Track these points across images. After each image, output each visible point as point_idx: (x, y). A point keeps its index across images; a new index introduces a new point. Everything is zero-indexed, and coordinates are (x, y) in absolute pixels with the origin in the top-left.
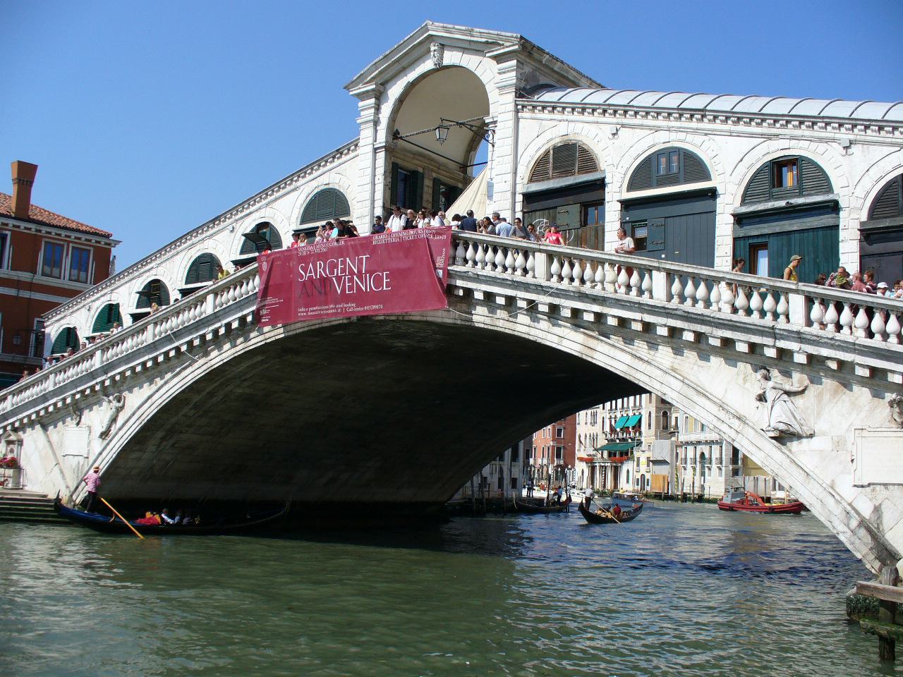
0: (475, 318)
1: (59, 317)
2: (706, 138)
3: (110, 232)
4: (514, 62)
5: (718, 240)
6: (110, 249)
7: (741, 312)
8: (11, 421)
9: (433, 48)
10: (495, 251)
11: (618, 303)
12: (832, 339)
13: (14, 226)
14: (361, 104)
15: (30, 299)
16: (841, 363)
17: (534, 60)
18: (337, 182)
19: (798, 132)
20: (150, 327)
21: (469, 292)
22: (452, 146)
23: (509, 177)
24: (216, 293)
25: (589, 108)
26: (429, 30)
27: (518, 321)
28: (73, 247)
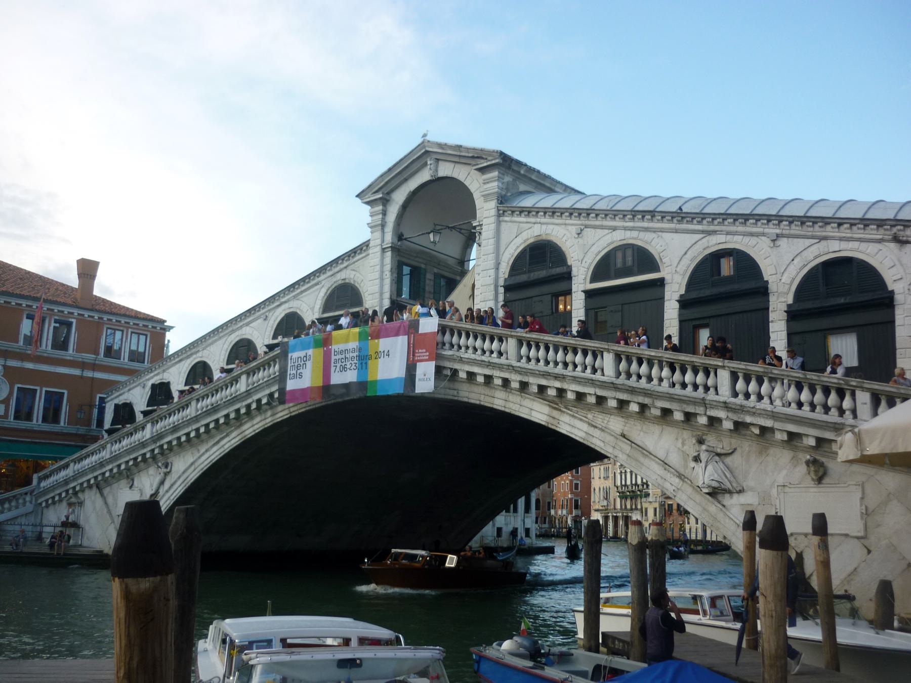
0: (462, 394)
1: (118, 394)
2: (652, 235)
3: (164, 318)
5: (666, 323)
6: (164, 336)
7: (677, 386)
8: (72, 485)
9: (429, 163)
10: (476, 338)
11: (575, 380)
12: (753, 408)
13: (79, 314)
15: (93, 379)
16: (764, 430)
17: (514, 171)
19: (733, 229)
20: (194, 403)
21: (455, 372)
22: (448, 246)
23: (492, 272)
24: (248, 373)
26: (424, 147)
27: (496, 395)
28: (132, 333)
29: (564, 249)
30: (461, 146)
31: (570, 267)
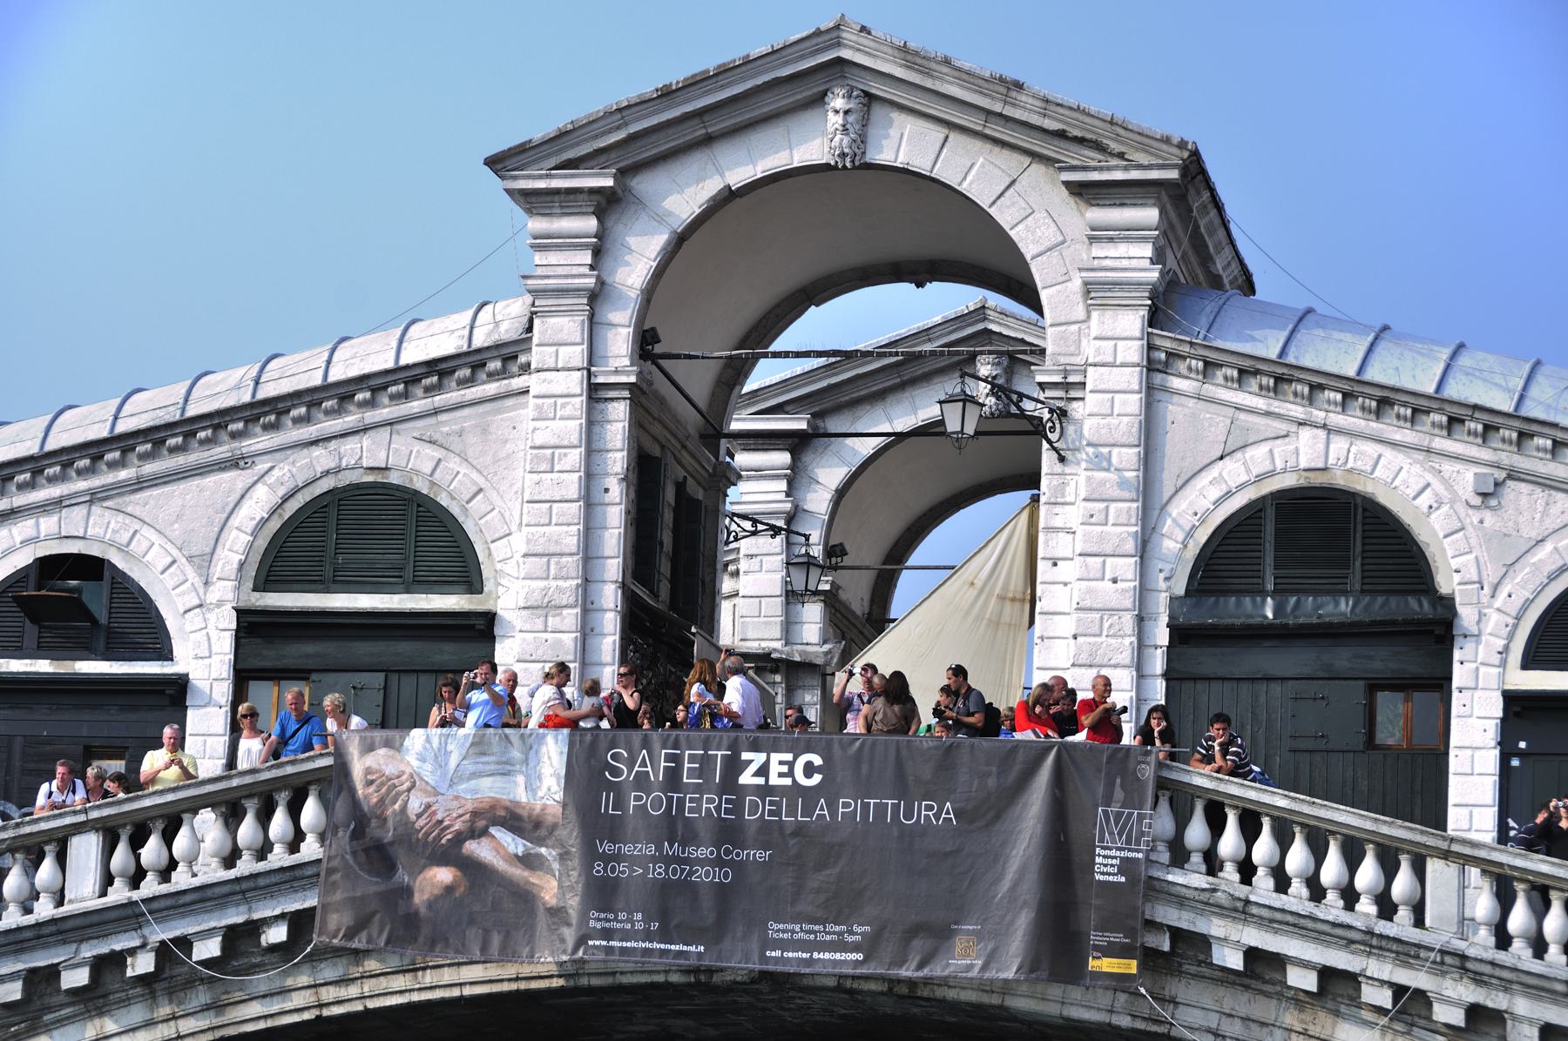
4: (1151, 215)
9: (838, 102)
10: (1283, 841)
14: (538, 224)
18: (428, 470)
23: (1126, 567)
25: (1405, 404)
26: (838, 44)
29: (1422, 534)
30: (1019, 86)
31: (1448, 603)
